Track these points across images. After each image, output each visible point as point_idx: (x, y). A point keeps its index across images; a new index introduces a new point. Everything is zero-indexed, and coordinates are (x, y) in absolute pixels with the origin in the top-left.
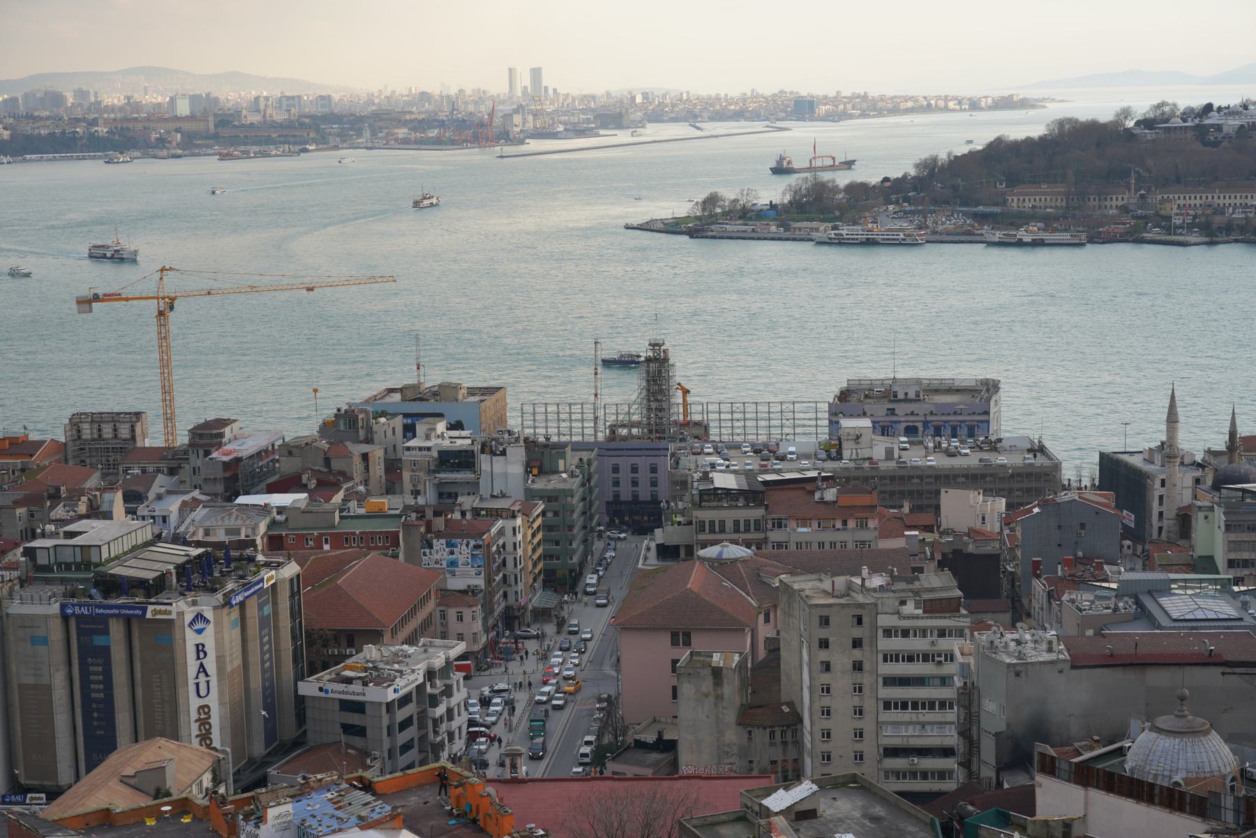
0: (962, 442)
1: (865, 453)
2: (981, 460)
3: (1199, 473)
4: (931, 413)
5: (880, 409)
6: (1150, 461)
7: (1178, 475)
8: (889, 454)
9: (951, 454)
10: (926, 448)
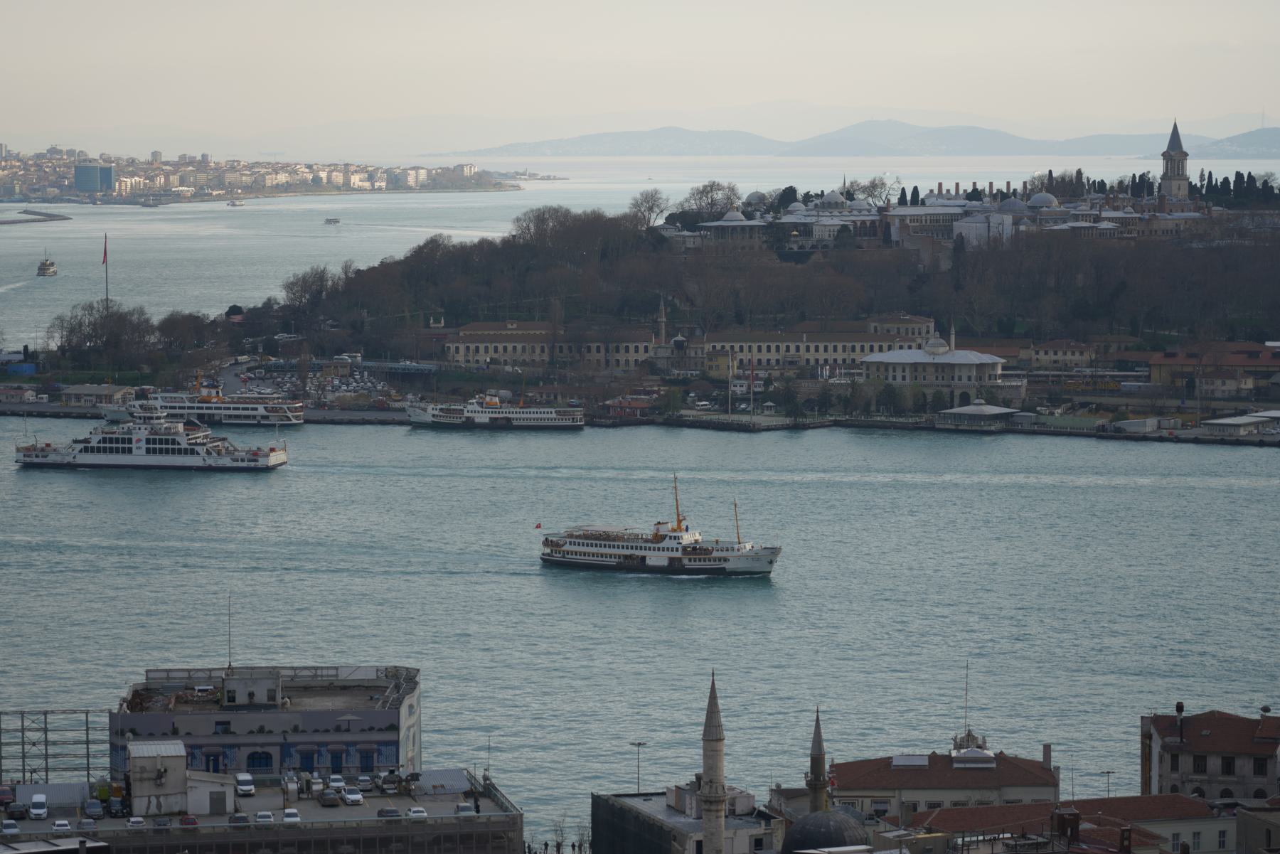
0: (349, 781)
1: (173, 803)
2: (380, 813)
3: (760, 830)
4: (296, 729)
5: (203, 723)
6: (677, 809)
7: (726, 834)
8: (217, 802)
9: (328, 803)
10: (285, 792)
